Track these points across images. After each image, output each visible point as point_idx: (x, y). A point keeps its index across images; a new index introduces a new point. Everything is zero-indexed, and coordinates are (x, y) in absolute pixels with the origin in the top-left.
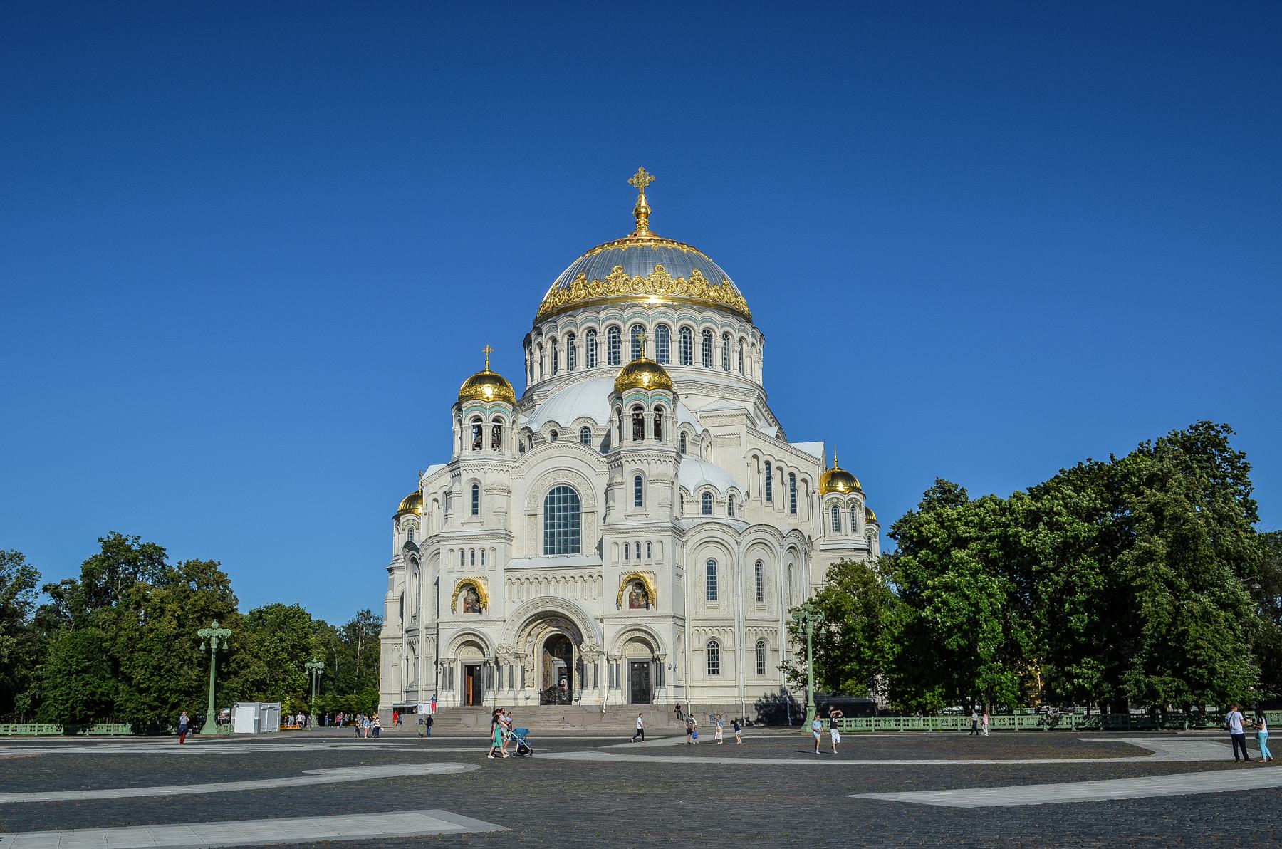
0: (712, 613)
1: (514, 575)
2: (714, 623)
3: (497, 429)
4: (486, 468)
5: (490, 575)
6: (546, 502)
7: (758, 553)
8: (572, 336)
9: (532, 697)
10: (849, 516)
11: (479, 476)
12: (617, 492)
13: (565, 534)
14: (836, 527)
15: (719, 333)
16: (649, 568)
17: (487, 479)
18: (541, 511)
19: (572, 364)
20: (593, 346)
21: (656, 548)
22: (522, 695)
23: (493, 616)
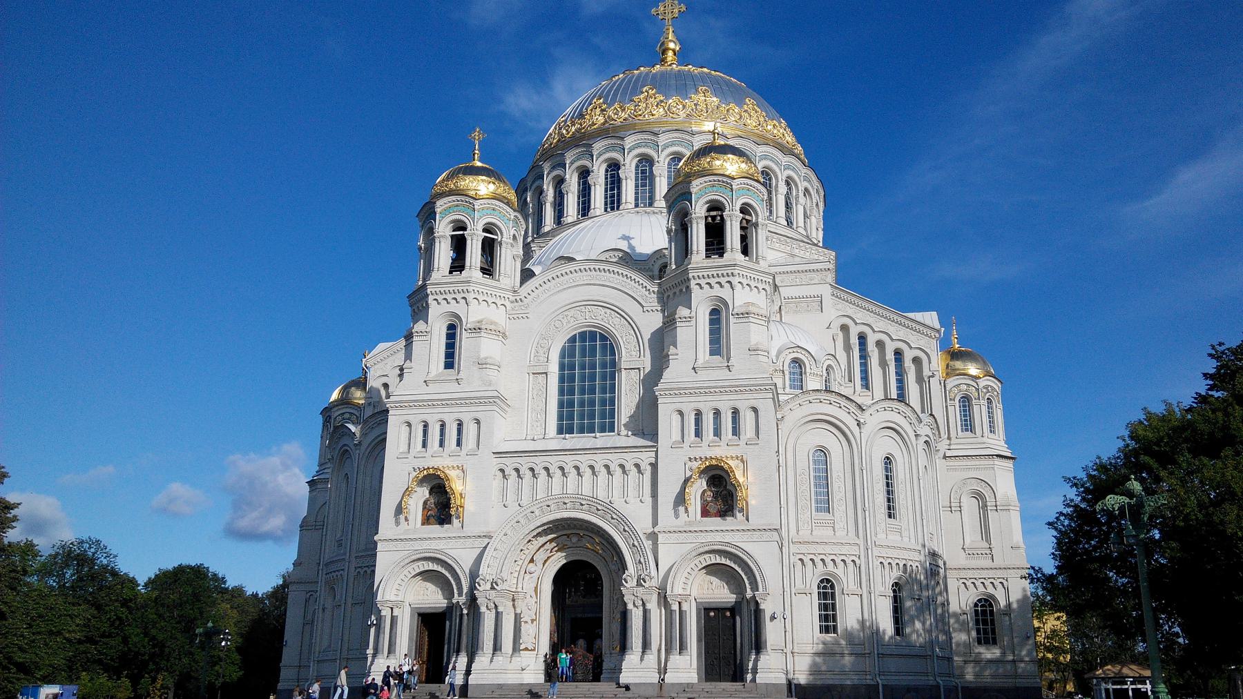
0: (823, 533)
1: (510, 463)
2: (828, 549)
3: (489, 247)
4: (470, 297)
5: (469, 463)
6: (562, 356)
7: (888, 445)
8: (584, 173)
9: (529, 669)
10: (984, 409)
11: (459, 309)
12: (683, 333)
13: (592, 403)
14: (968, 425)
15: (782, 176)
16: (733, 452)
17: (473, 314)
18: (554, 368)
19: (585, 209)
20: (614, 182)
21: (747, 419)
22: (519, 661)
23: (468, 530)
